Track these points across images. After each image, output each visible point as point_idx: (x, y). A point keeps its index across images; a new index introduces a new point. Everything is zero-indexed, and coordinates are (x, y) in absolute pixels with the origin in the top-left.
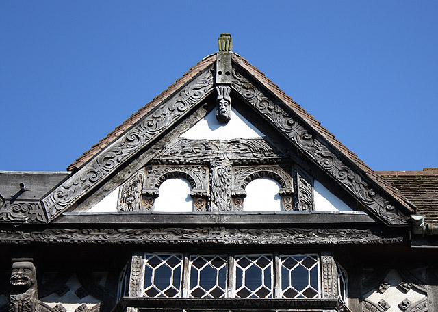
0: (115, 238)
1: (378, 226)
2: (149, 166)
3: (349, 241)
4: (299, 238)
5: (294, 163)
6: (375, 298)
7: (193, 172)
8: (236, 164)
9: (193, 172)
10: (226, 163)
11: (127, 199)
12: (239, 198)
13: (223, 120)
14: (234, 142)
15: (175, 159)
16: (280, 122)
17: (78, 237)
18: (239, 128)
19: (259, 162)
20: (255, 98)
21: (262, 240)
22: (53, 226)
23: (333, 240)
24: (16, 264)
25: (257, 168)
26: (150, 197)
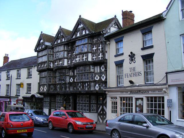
0: (74, 40)
2: (76, 31)
6: (94, 40)
8: (82, 29)
11: (75, 36)
12: (82, 33)
13: (80, 25)
17: (72, 41)
22: (71, 40)
26: (77, 35)
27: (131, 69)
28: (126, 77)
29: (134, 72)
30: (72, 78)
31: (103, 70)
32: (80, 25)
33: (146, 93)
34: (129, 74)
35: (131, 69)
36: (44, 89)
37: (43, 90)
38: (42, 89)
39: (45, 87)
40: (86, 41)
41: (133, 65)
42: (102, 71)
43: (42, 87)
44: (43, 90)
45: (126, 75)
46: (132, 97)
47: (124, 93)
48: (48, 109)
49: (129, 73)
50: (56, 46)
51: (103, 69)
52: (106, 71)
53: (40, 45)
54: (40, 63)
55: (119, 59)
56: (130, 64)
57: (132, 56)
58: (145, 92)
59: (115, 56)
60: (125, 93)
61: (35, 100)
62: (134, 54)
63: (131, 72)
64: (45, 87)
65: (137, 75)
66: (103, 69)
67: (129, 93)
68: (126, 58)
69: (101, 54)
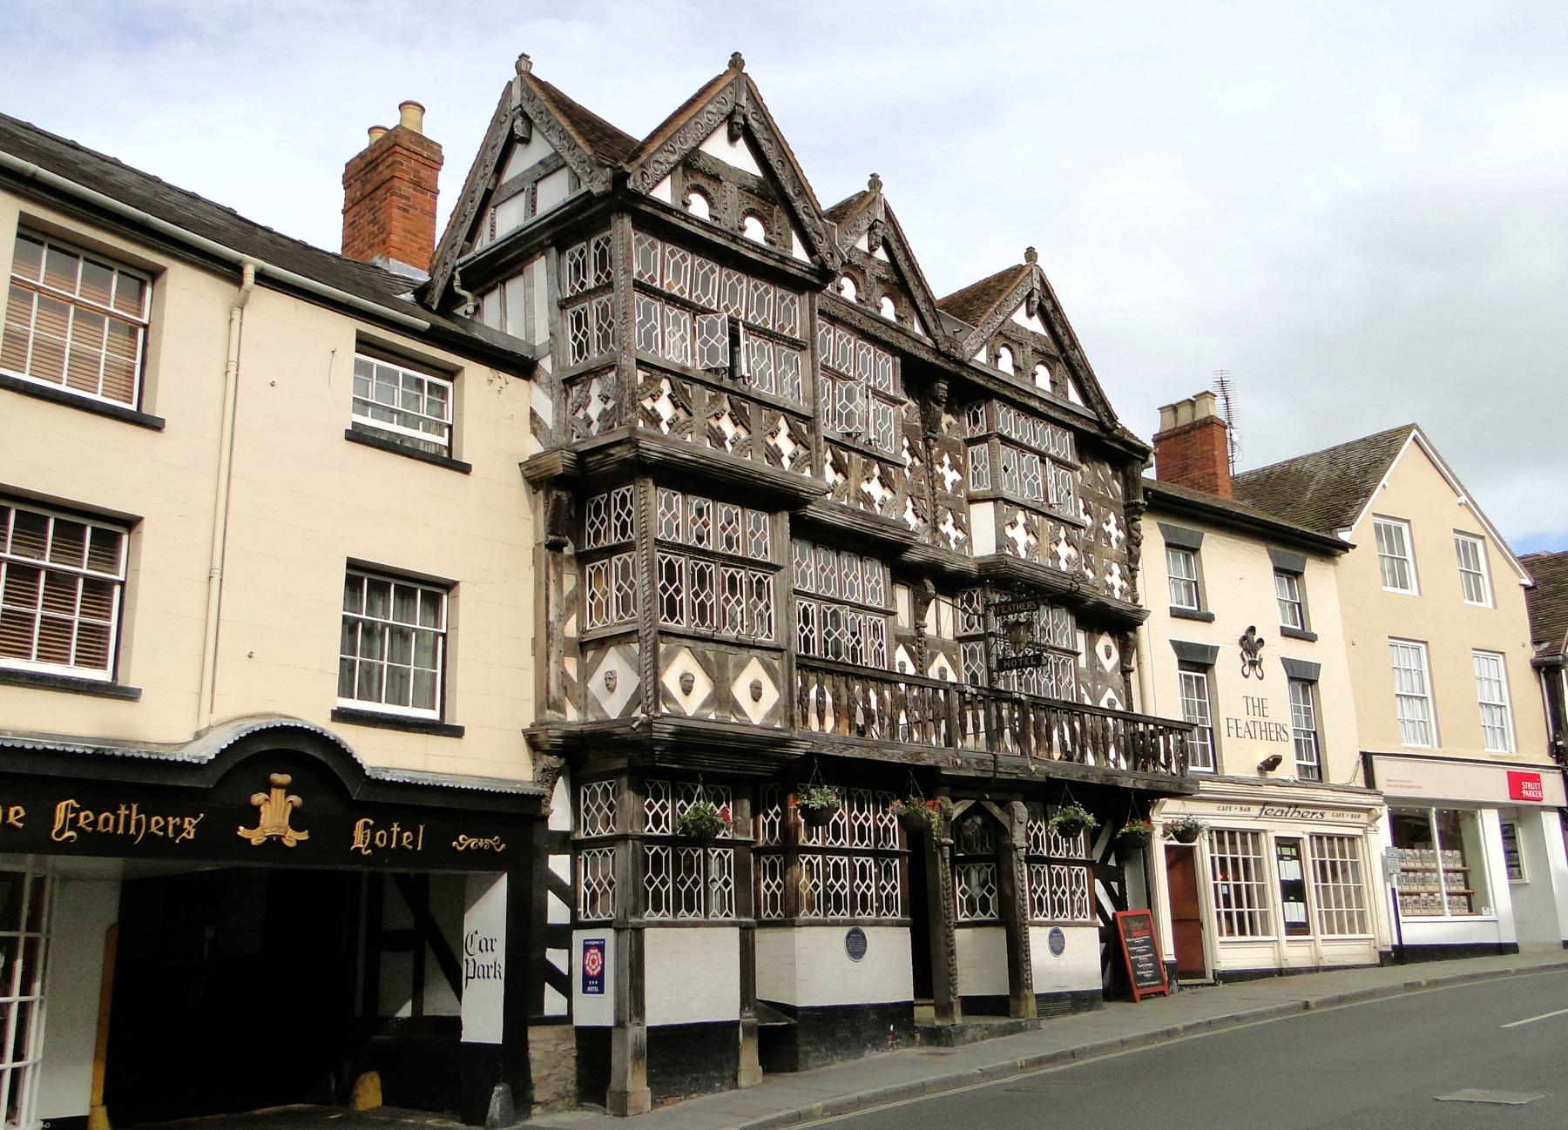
0: (990, 385)
1: (1100, 424)
3: (1086, 428)
4: (1067, 419)
5: (1059, 361)
7: (1015, 347)
9: (1015, 347)
10: (1030, 349)
14: (1033, 333)
15: (1008, 334)
16: (1060, 331)
18: (1036, 325)
19: (1043, 353)
20: (1048, 305)
21: (1052, 413)
23: (1078, 424)
24: (941, 385)
25: (1047, 360)
27: (1250, 701)
28: (1233, 732)
29: (1262, 720)
30: (901, 654)
31: (1110, 663)
32: (1030, 315)
33: (1314, 817)
34: (1242, 724)
35: (1250, 701)
36: (741, 691)
37: (722, 698)
38: (702, 688)
39: (754, 671)
40: (1062, 445)
41: (1252, 686)
42: (1102, 666)
43: (681, 665)
44: (722, 698)
45: (1232, 723)
46: (1256, 834)
47: (1233, 812)
48: (736, 931)
49: (1244, 718)
50: (841, 312)
51: (1108, 655)
52: (1126, 672)
53: (702, 182)
54: (680, 377)
55: (1193, 633)
56: (1261, 678)
57: (1250, 644)
58: (1314, 814)
59: (1177, 614)
60: (1238, 812)
61: (297, 821)
62: (1261, 641)
63: (1251, 717)
64: (754, 671)
65: (1274, 736)
66: (1108, 655)
67: (1255, 810)
68: (1276, 650)
69: (1115, 568)
